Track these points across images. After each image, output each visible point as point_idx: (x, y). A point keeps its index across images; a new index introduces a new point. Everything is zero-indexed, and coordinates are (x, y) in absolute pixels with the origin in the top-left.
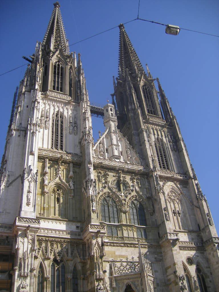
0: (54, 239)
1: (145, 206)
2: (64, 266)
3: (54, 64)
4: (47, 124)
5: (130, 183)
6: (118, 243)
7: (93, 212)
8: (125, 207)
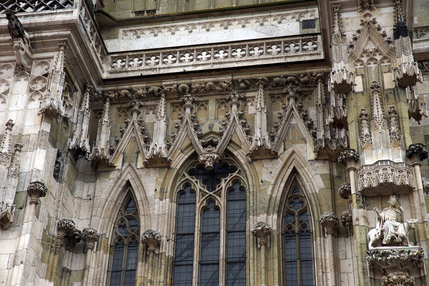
0: (183, 83)
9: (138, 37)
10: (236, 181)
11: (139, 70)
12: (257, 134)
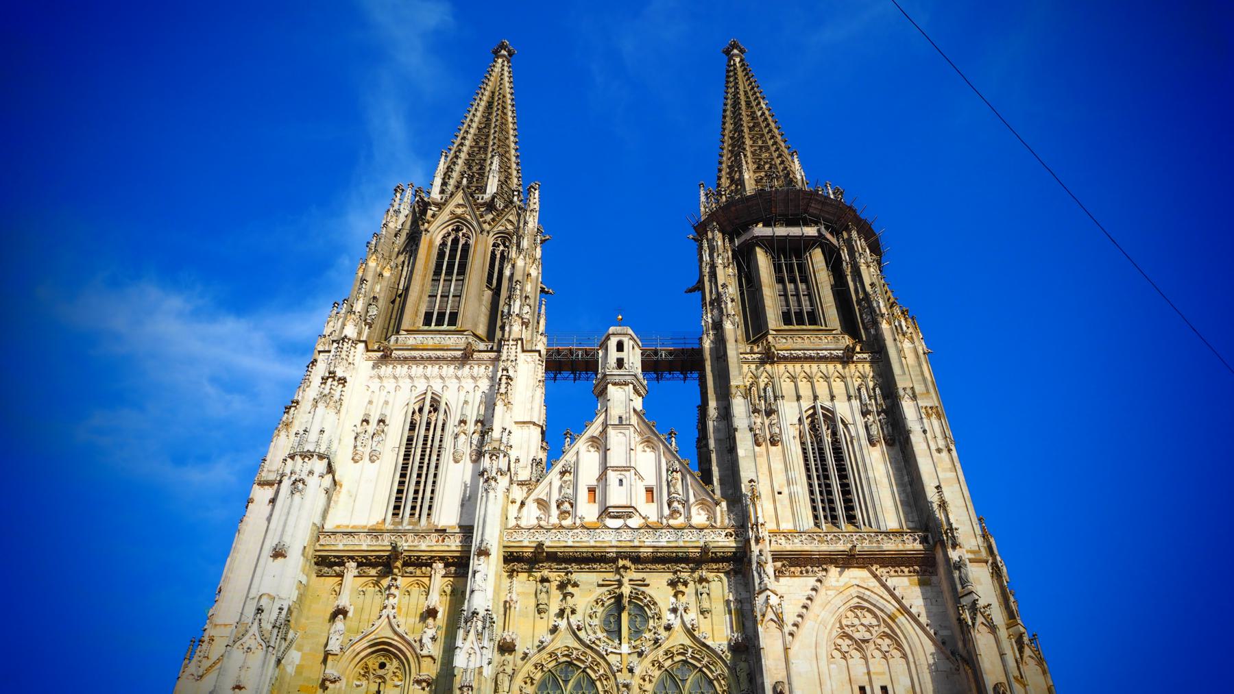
3: (438, 241)
4: (374, 444)
5: (660, 604)
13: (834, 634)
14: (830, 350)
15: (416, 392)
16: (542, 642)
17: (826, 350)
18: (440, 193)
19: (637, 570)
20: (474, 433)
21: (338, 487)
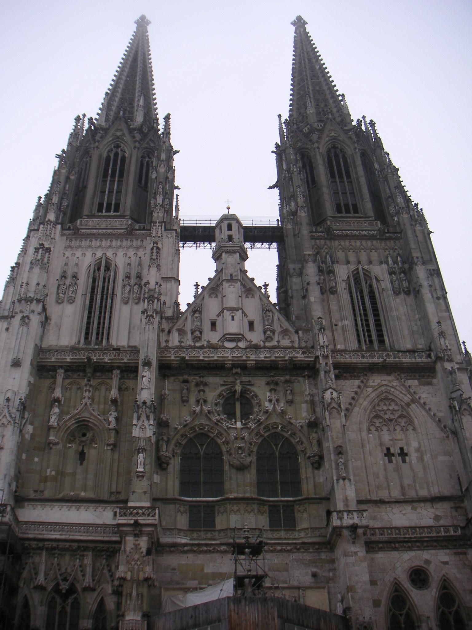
0: (55, 544)
1: (299, 448)
2: (79, 604)
3: (105, 155)
5: (261, 397)
6: (212, 544)
7: (138, 477)
8: (242, 455)
9: (34, 509)
10: (76, 598)
11: (34, 534)
12: (87, 580)
13: (372, 415)
14: (369, 230)
15: (96, 257)
16: (186, 421)
17: (366, 230)
18: (106, 121)
19: (245, 375)
20: (135, 285)
21: (49, 321)
